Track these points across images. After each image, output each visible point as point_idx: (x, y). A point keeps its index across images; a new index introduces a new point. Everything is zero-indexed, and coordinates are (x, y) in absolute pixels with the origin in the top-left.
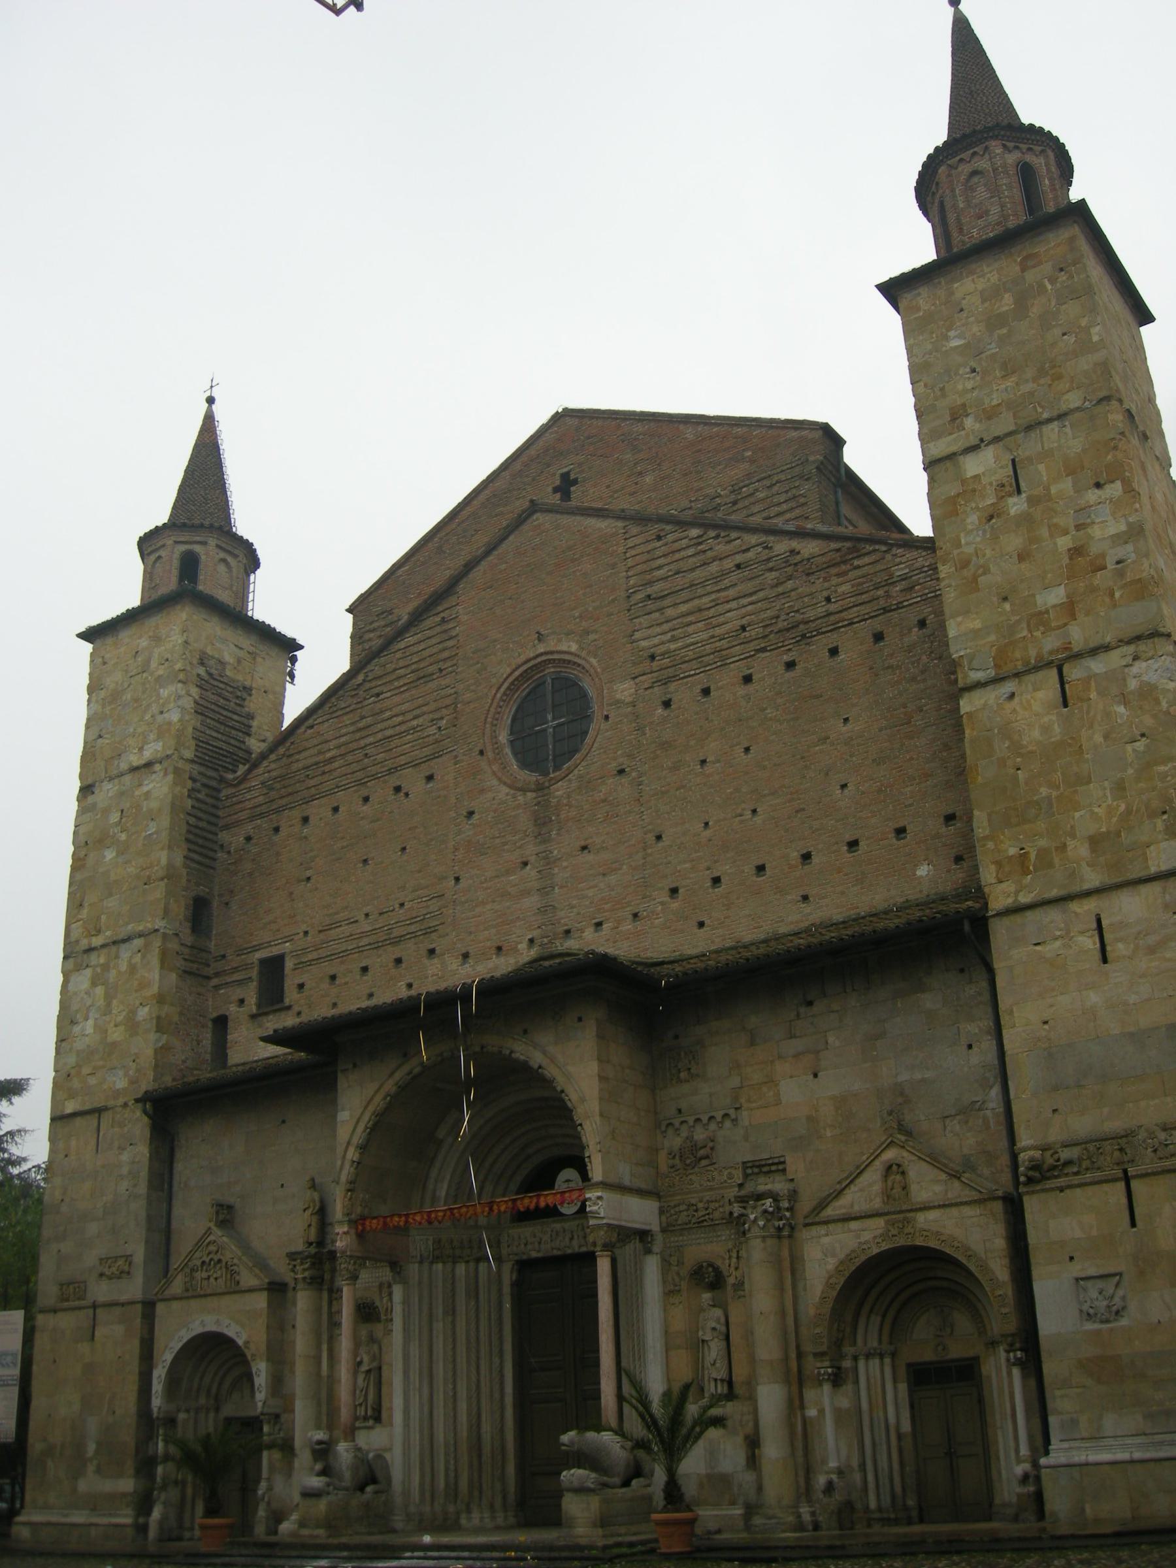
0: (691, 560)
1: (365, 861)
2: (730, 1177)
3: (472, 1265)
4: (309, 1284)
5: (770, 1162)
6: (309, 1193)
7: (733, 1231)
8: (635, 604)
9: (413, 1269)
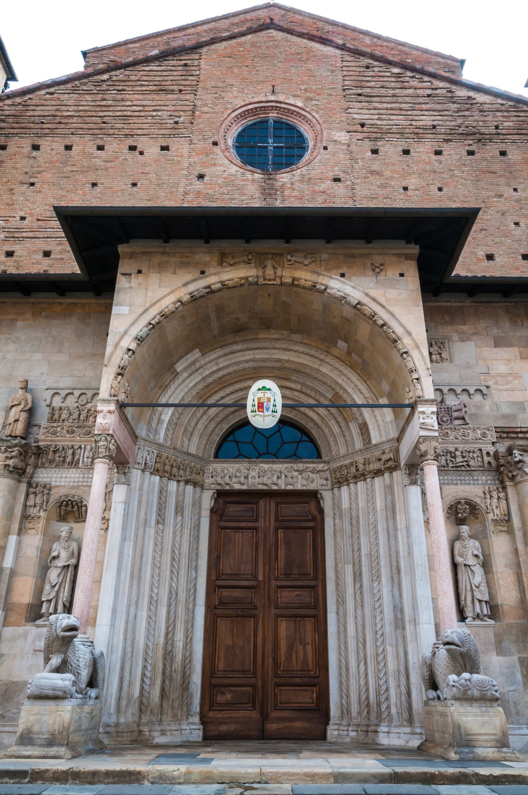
0: (392, 84)
1: (94, 185)
2: (484, 435)
4: (11, 472)
5: (519, 430)
6: (21, 392)
7: (489, 477)
8: (349, 95)
9: (136, 474)
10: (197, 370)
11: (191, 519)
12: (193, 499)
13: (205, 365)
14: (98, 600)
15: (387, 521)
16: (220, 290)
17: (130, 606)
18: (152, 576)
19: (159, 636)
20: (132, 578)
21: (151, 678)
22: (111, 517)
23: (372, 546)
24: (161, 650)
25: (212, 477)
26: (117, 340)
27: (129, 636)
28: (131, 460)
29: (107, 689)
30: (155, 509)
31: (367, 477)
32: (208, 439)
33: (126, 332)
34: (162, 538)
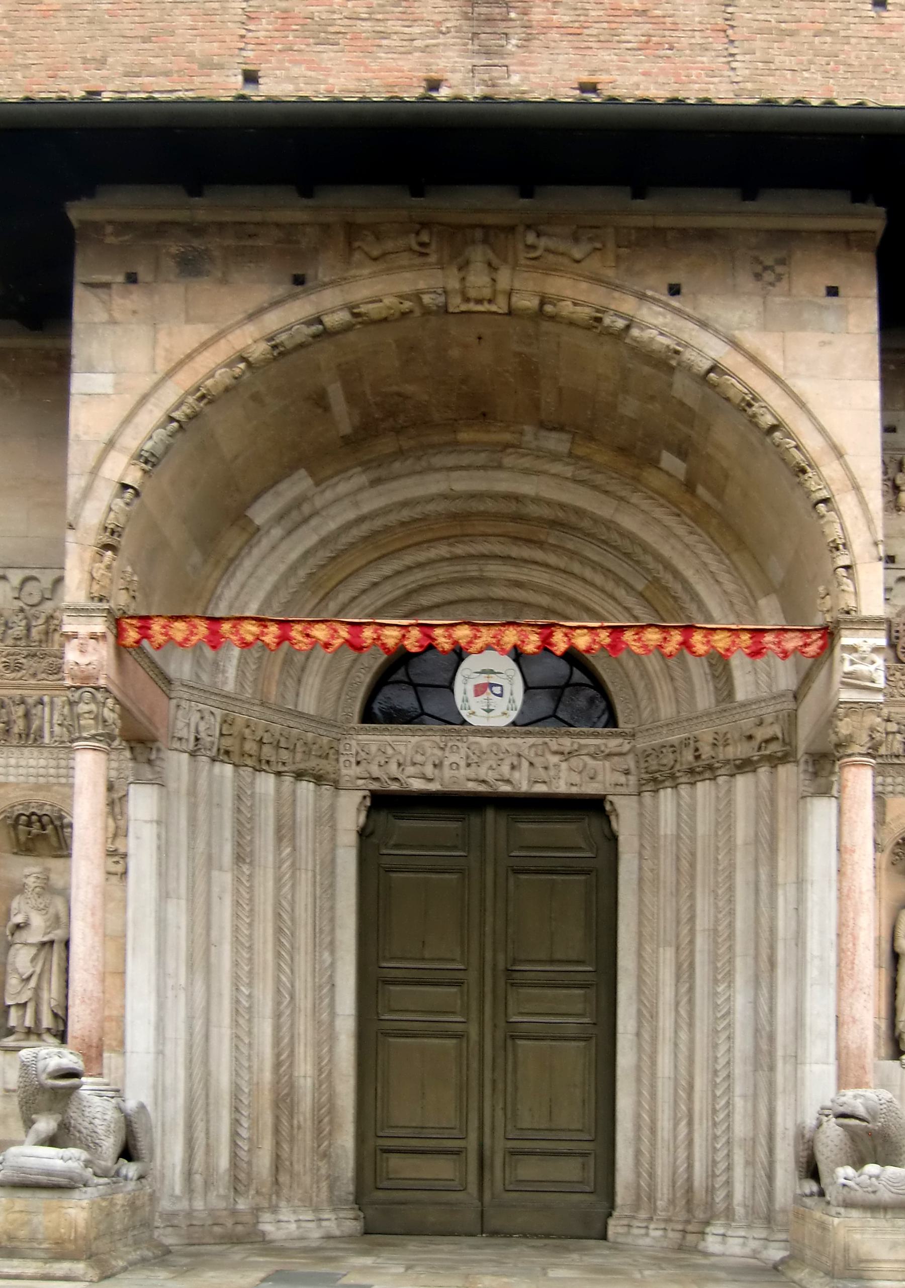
3: (288, 780)
10: (306, 520)
11: (314, 852)
12: (317, 809)
13: (324, 507)
14: (123, 1007)
15: (756, 868)
16: (347, 328)
17: (193, 1018)
18: (236, 964)
19: (261, 1070)
20: (190, 966)
21: (250, 1140)
22: (131, 851)
23: (720, 916)
24: (267, 1093)
25: (358, 763)
26: (91, 462)
27: (198, 1071)
28: (161, 733)
29: (163, 1158)
30: (228, 833)
31: (719, 772)
32: (344, 680)
33: (111, 444)
34: (251, 889)
